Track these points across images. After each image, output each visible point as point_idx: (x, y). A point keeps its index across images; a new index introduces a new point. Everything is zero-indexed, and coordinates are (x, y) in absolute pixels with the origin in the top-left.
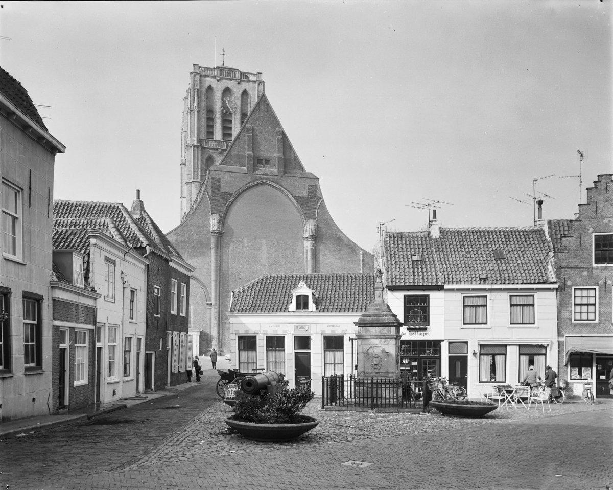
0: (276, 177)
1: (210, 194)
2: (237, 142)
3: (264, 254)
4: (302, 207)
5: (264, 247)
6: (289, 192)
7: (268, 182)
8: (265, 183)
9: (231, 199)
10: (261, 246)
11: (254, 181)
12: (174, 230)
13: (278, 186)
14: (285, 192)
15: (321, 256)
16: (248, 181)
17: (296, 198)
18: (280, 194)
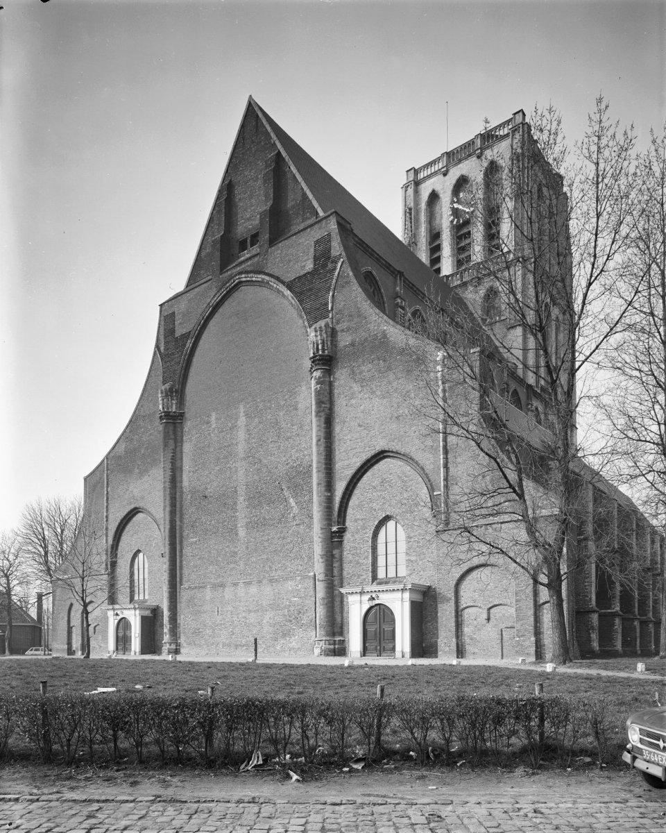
0: (256, 259)
1: (162, 349)
2: (210, 228)
3: (241, 435)
4: (301, 302)
5: (242, 420)
6: (278, 279)
7: (243, 278)
8: (240, 282)
9: (189, 344)
10: (237, 419)
11: (221, 289)
12: (123, 434)
13: (260, 277)
14: (274, 283)
15: (342, 406)
16: (215, 290)
17: (290, 286)
18: (265, 291)
